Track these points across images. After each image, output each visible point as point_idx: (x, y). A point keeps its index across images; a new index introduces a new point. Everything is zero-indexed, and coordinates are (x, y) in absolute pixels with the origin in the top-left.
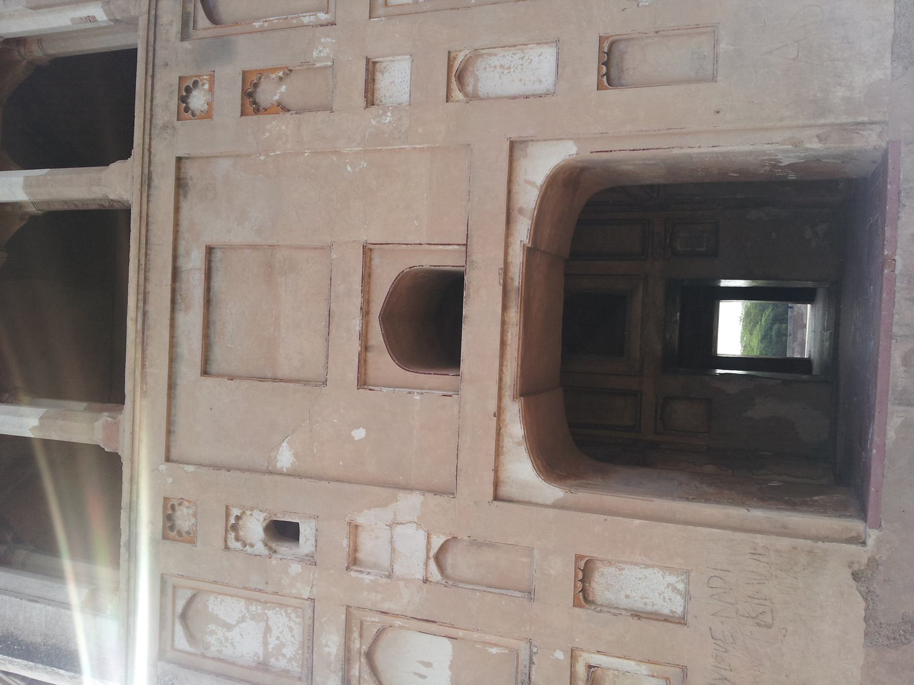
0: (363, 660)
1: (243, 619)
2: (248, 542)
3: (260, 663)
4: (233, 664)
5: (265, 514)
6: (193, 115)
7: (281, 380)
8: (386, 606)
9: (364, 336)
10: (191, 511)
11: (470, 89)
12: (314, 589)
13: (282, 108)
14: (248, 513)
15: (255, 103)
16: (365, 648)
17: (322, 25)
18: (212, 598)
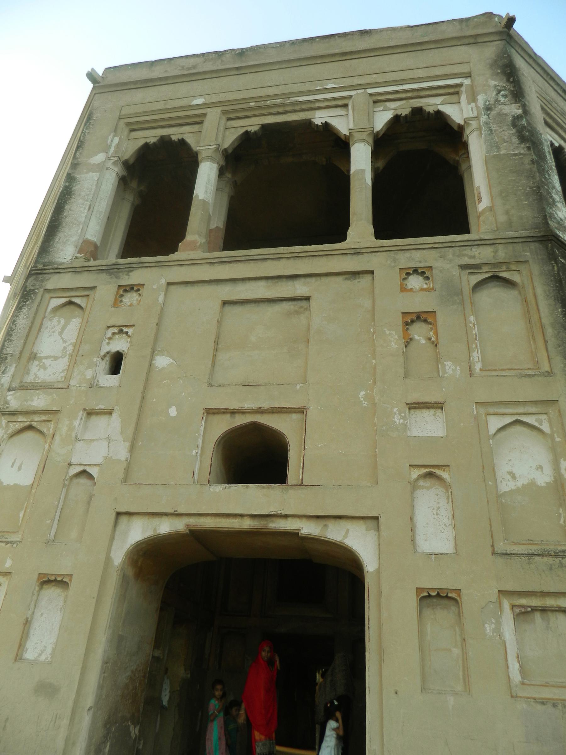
0: (28, 423)
1: (65, 342)
2: (111, 342)
3: (36, 355)
4: (36, 338)
5: (126, 351)
6: (405, 279)
7: (215, 355)
8: (57, 437)
9: (242, 412)
10: (134, 302)
11: (421, 483)
12: (75, 388)
14: (129, 340)
15: (413, 321)
16: (34, 424)
17: (470, 367)
18: (80, 320)
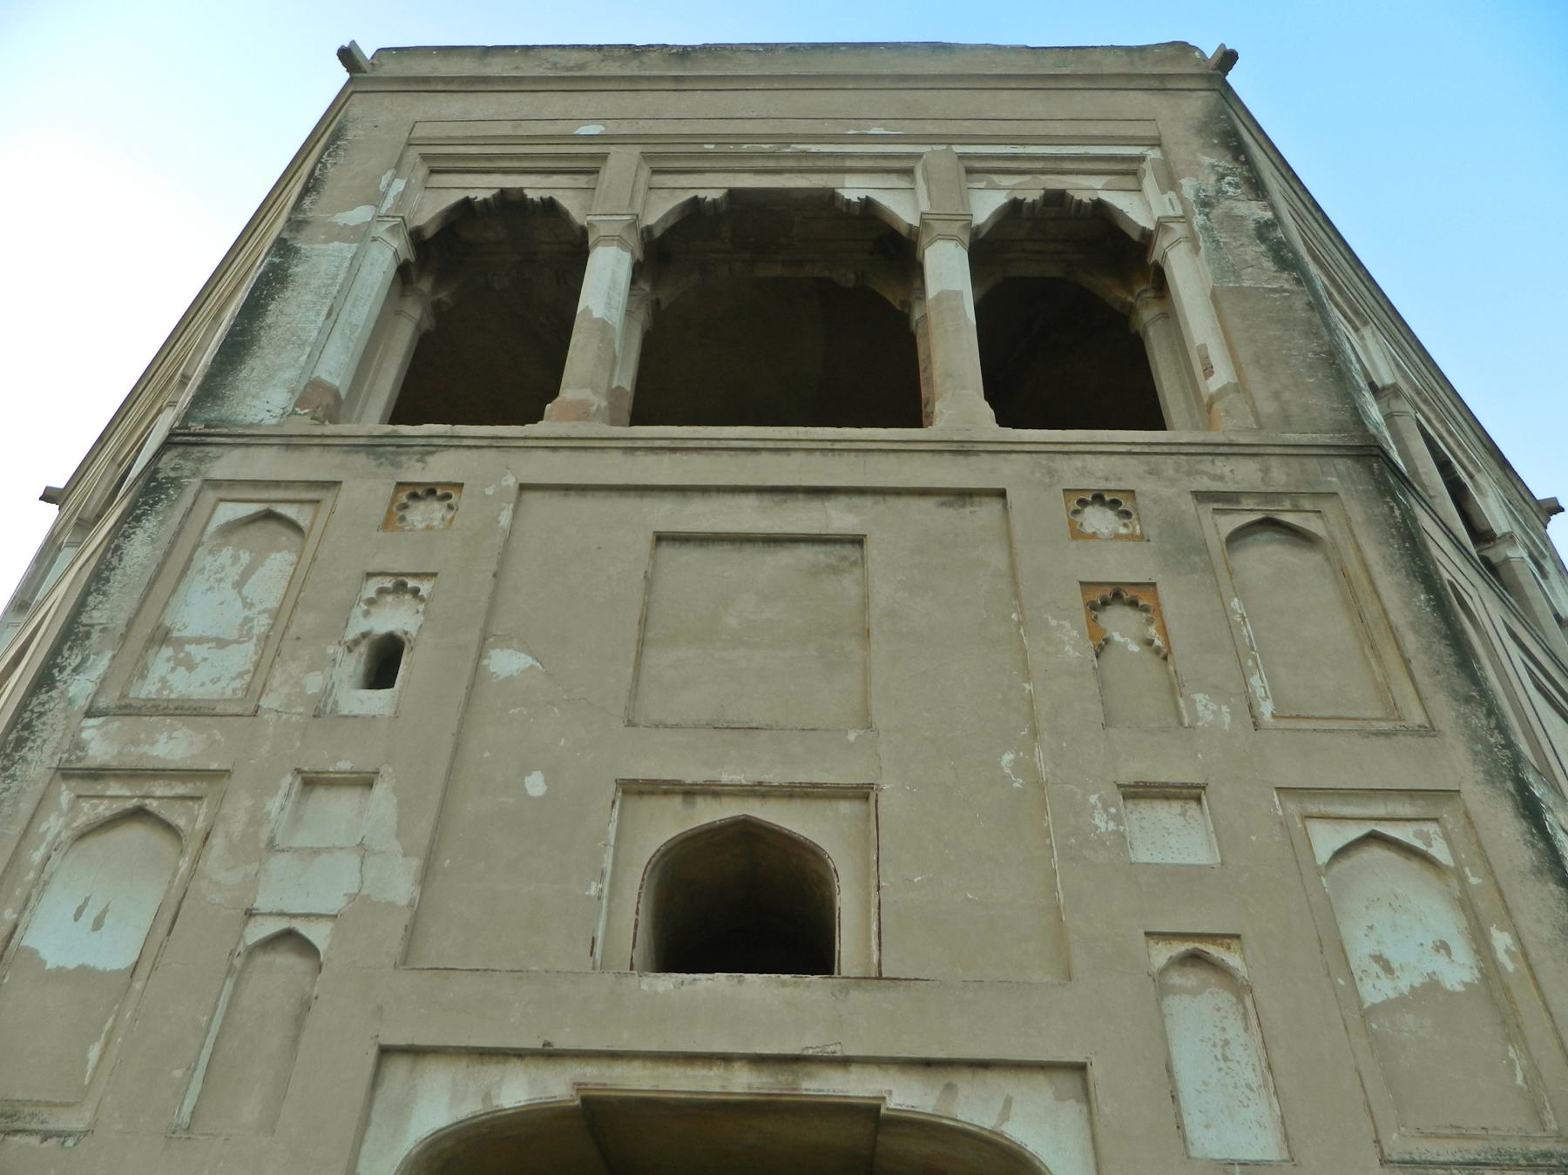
0: (135, 802)
1: (248, 605)
2: (373, 610)
3: (168, 632)
4: (174, 591)
5: (414, 633)
6: (1076, 512)
7: (639, 654)
8: (217, 841)
9: (713, 791)
10: (435, 523)
11: (1175, 978)
12: (274, 716)
13: (1102, 646)
14: (421, 607)
15: (1105, 603)
16: (152, 805)
17: (1250, 707)
18: (293, 558)
